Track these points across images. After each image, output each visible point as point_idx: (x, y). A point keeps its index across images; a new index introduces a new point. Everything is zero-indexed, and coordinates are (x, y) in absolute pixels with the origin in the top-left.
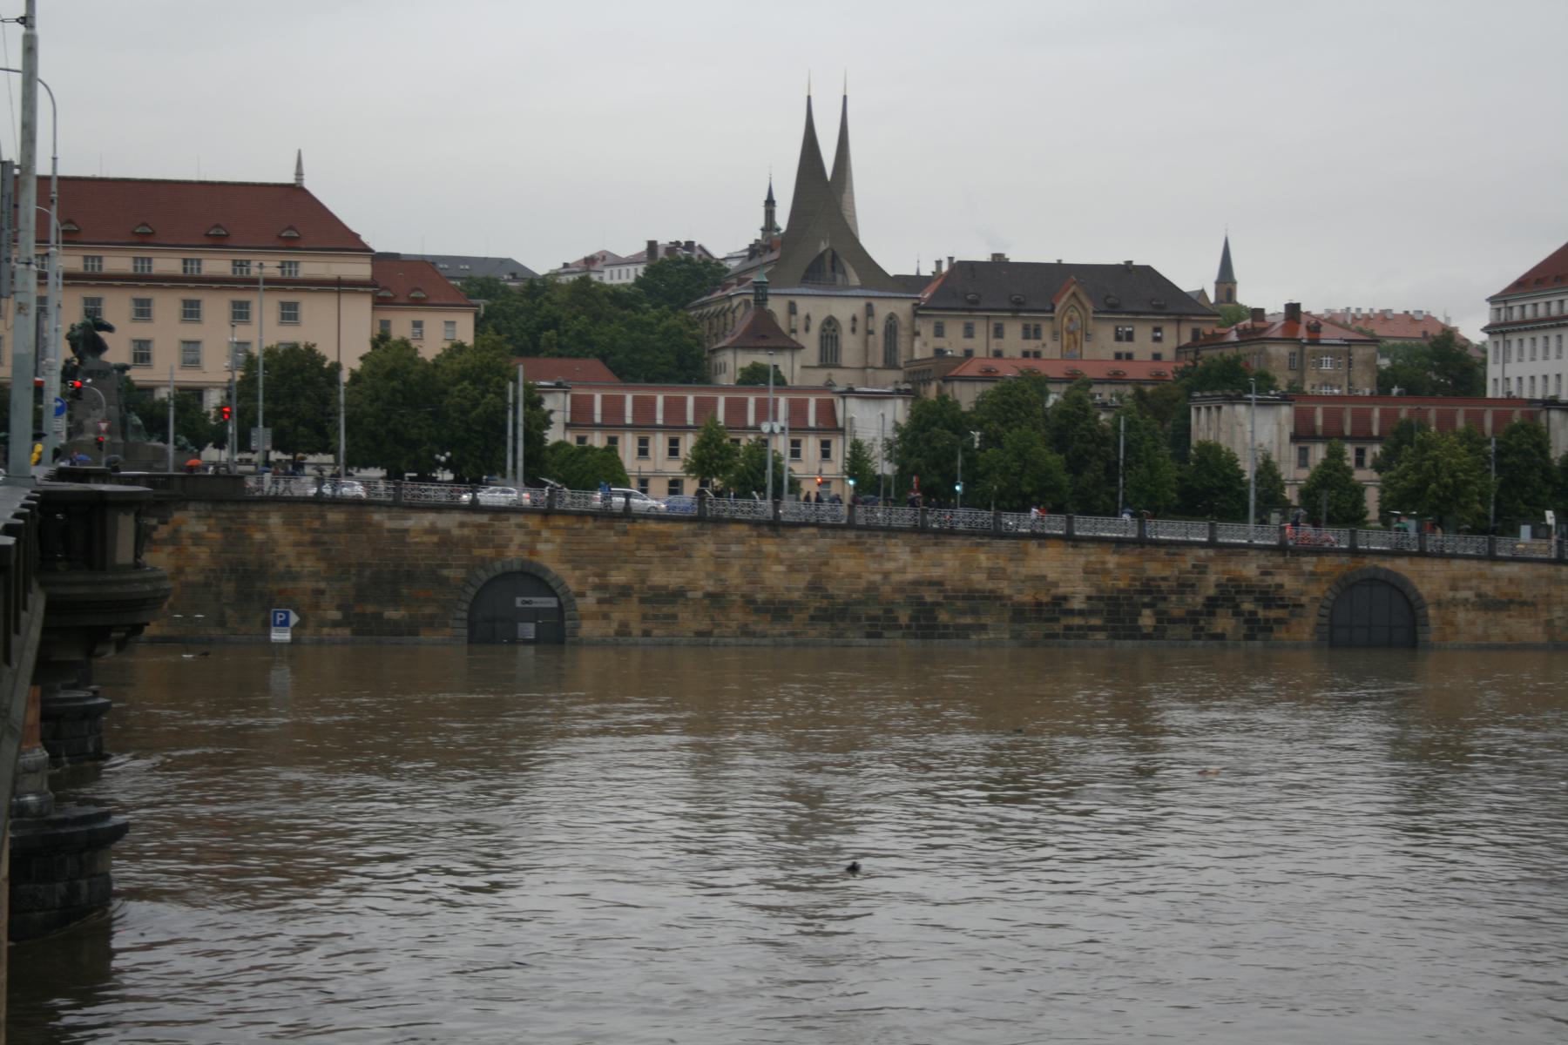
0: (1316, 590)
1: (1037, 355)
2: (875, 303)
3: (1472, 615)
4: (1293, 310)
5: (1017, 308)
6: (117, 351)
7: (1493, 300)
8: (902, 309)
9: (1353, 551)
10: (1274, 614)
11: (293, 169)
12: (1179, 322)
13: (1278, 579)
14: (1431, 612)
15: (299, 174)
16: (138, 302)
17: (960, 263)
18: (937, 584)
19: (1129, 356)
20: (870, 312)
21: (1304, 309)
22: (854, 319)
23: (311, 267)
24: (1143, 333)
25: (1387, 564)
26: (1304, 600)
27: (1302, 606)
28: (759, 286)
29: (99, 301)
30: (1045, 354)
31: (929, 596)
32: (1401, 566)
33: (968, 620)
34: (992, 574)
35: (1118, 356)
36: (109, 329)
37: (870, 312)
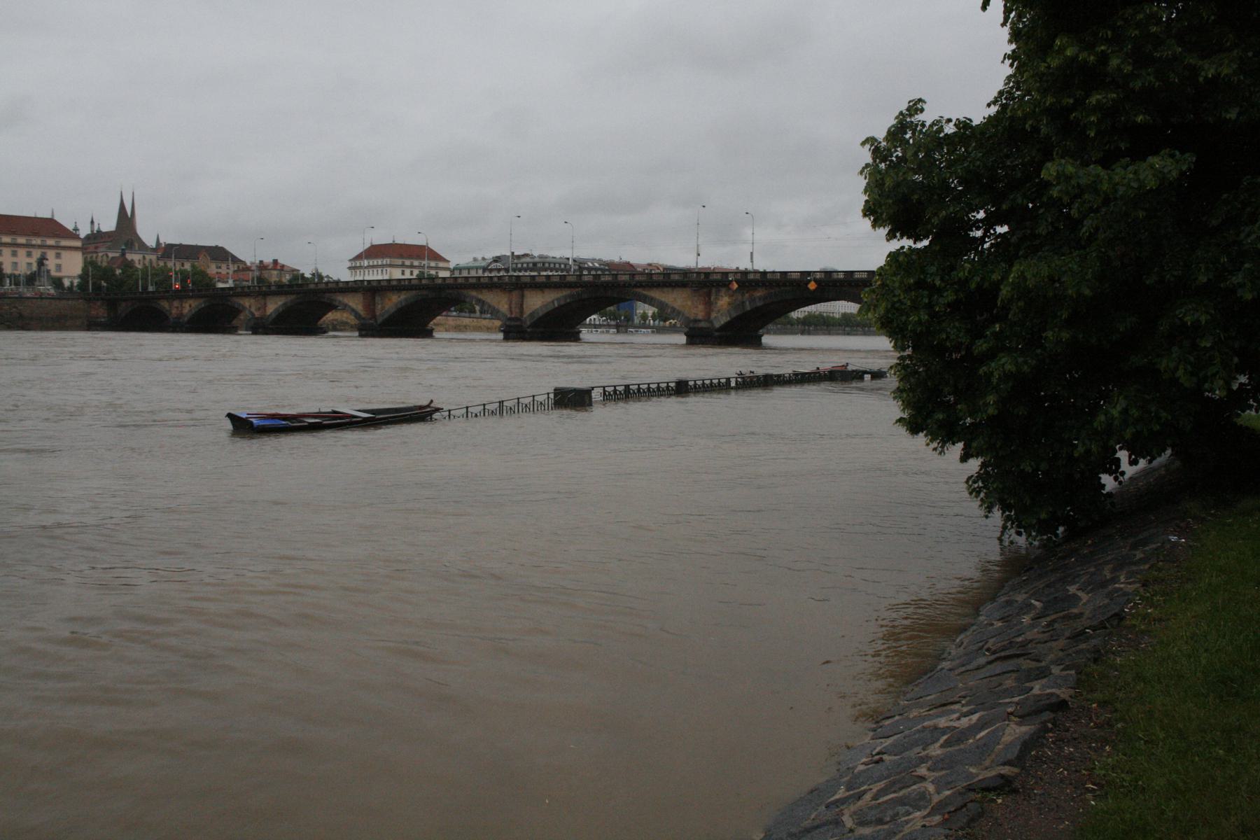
4: (275, 262)
6: (51, 263)
7: (350, 260)
8: (154, 257)
11: (51, 212)
15: (53, 215)
16: (13, 251)
18: (336, 320)
19: (220, 273)
20: (144, 258)
21: (279, 261)
22: (139, 260)
23: (64, 243)
24: (224, 266)
28: (123, 250)
29: (45, 253)
31: (335, 323)
33: (342, 328)
34: (347, 318)
36: (47, 259)
37: (144, 258)
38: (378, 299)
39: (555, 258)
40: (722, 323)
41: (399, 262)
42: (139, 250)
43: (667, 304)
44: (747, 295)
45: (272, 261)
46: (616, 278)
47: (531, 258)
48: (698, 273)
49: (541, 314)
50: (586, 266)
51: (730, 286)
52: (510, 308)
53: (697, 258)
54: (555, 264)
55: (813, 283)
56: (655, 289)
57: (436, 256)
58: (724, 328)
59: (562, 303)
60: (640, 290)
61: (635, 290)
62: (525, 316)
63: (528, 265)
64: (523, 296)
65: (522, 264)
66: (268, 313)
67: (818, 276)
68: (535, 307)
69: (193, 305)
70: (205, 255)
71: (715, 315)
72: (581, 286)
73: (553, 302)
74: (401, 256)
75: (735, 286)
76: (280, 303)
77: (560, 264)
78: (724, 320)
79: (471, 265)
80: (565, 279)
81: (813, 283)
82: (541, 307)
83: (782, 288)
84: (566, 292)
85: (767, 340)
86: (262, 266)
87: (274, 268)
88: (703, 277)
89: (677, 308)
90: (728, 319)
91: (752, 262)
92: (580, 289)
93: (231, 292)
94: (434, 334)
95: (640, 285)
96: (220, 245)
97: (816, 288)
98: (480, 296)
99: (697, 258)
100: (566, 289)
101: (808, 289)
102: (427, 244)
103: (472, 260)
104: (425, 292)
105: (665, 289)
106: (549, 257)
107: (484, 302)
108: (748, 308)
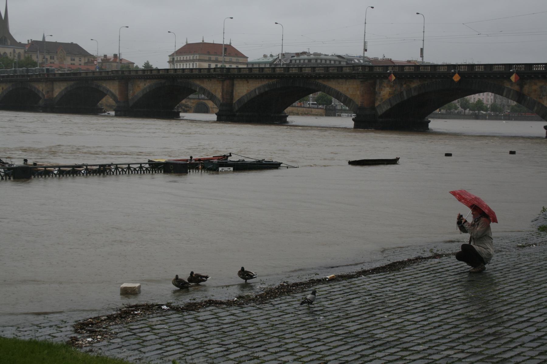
0: (194, 105)
1: (53, 63)
2: (16, 49)
3: (216, 110)
5: (48, 52)
7: (169, 56)
8: (22, 51)
9: (199, 99)
10: (187, 109)
12: (85, 57)
13: (188, 103)
14: (210, 109)
17: (34, 41)
19: (74, 64)
20: (14, 52)
22: (11, 53)
24: (77, 59)
25: (204, 101)
26: (192, 107)
27: (191, 108)
30: (55, 63)
32: (206, 102)
35: (72, 64)
37: (14, 52)
38: (130, 85)
39: (327, 55)
40: (384, 110)
41: (207, 57)
42: (11, 45)
43: (341, 94)
44: (404, 86)
45: (103, 56)
46: (301, 71)
47: (308, 55)
48: (364, 67)
49: (246, 101)
50: (353, 62)
51: (389, 78)
52: (223, 95)
53: (364, 53)
54: (326, 60)
55: (457, 75)
56: (332, 80)
57: (238, 54)
58: (387, 114)
59: (262, 91)
60: (320, 81)
61: (317, 81)
62: (234, 102)
63: (304, 62)
64: (233, 85)
65: (300, 60)
66: (55, 96)
67: (462, 70)
68: (242, 95)
69: (5, 88)
70: (62, 50)
71: (379, 103)
72: (274, 78)
73: (255, 90)
74: (209, 53)
75: (393, 78)
76: (63, 88)
77: (330, 60)
78: (386, 108)
79: (261, 60)
80: (263, 71)
81: (457, 75)
82: (246, 95)
83: (434, 80)
84: (265, 82)
85: (434, 124)
86: (105, 59)
87: (115, 61)
88: (367, 70)
89: (349, 96)
90: (389, 107)
91: (422, 55)
92: (275, 80)
93: (29, 79)
94: (181, 114)
95: (319, 77)
96: (74, 43)
97: (460, 81)
98: (202, 85)
99: (364, 53)
100: (265, 80)
101: (453, 80)
102: (230, 43)
103: (262, 56)
104: (163, 81)
105: (340, 81)
106: (323, 55)
107: (205, 89)
108: (406, 98)
